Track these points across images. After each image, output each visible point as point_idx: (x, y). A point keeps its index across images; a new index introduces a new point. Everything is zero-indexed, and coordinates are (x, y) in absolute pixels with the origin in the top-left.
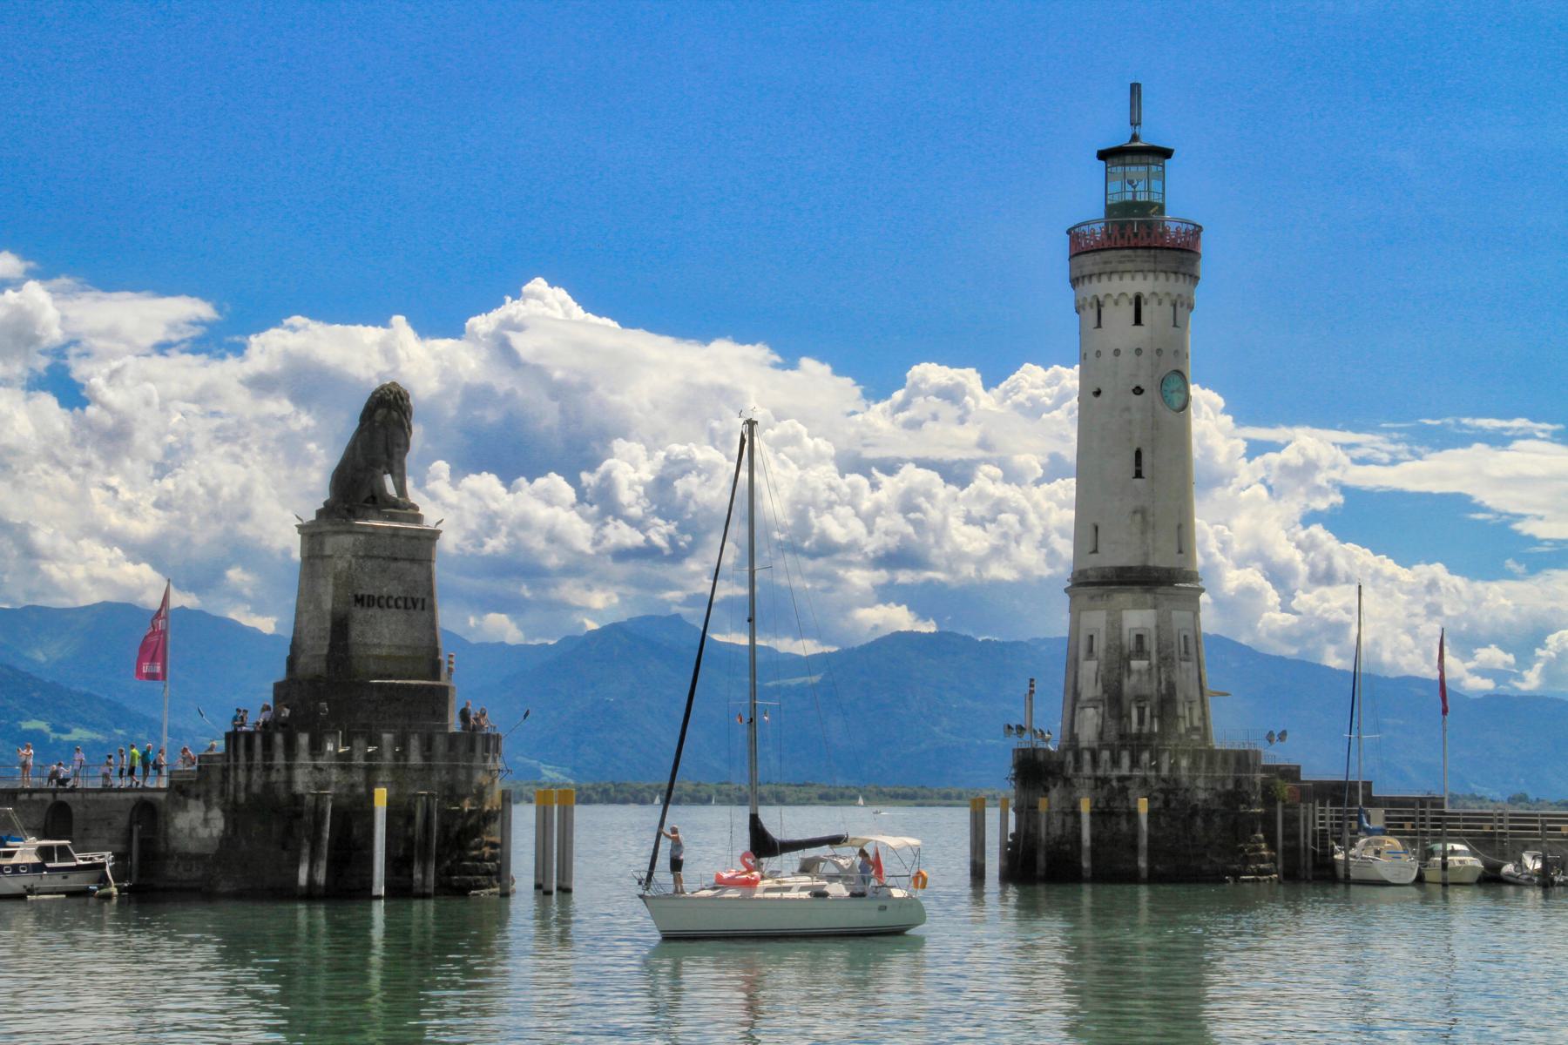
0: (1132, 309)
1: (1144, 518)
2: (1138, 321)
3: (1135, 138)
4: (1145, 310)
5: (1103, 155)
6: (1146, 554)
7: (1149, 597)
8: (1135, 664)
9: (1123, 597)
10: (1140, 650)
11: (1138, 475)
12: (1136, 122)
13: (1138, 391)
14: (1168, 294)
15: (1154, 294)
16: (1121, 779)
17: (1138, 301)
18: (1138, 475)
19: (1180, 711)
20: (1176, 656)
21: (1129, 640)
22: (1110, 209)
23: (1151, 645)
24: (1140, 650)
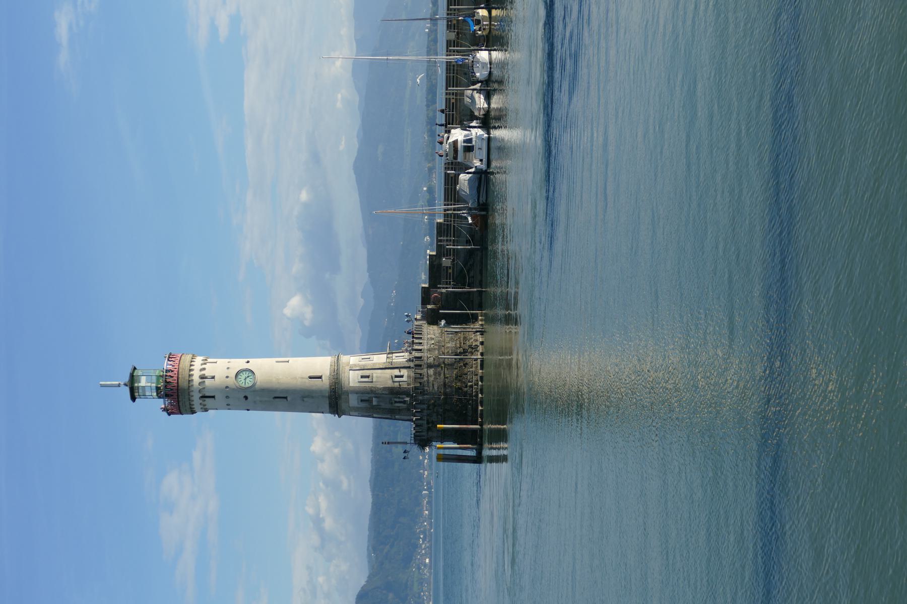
0: (207, 399)
1: (308, 397)
2: (213, 397)
3: (125, 385)
4: (207, 394)
5: (133, 399)
6: (323, 396)
7: (343, 397)
8: (375, 403)
9: (343, 406)
10: (369, 401)
11: (286, 398)
12: (119, 385)
13: (246, 398)
14: (200, 384)
15: (200, 391)
16: (428, 423)
17: (204, 397)
18: (286, 398)
19: (397, 385)
20: (370, 385)
21: (364, 405)
22: (160, 397)
23: (366, 397)
24: (369, 401)
